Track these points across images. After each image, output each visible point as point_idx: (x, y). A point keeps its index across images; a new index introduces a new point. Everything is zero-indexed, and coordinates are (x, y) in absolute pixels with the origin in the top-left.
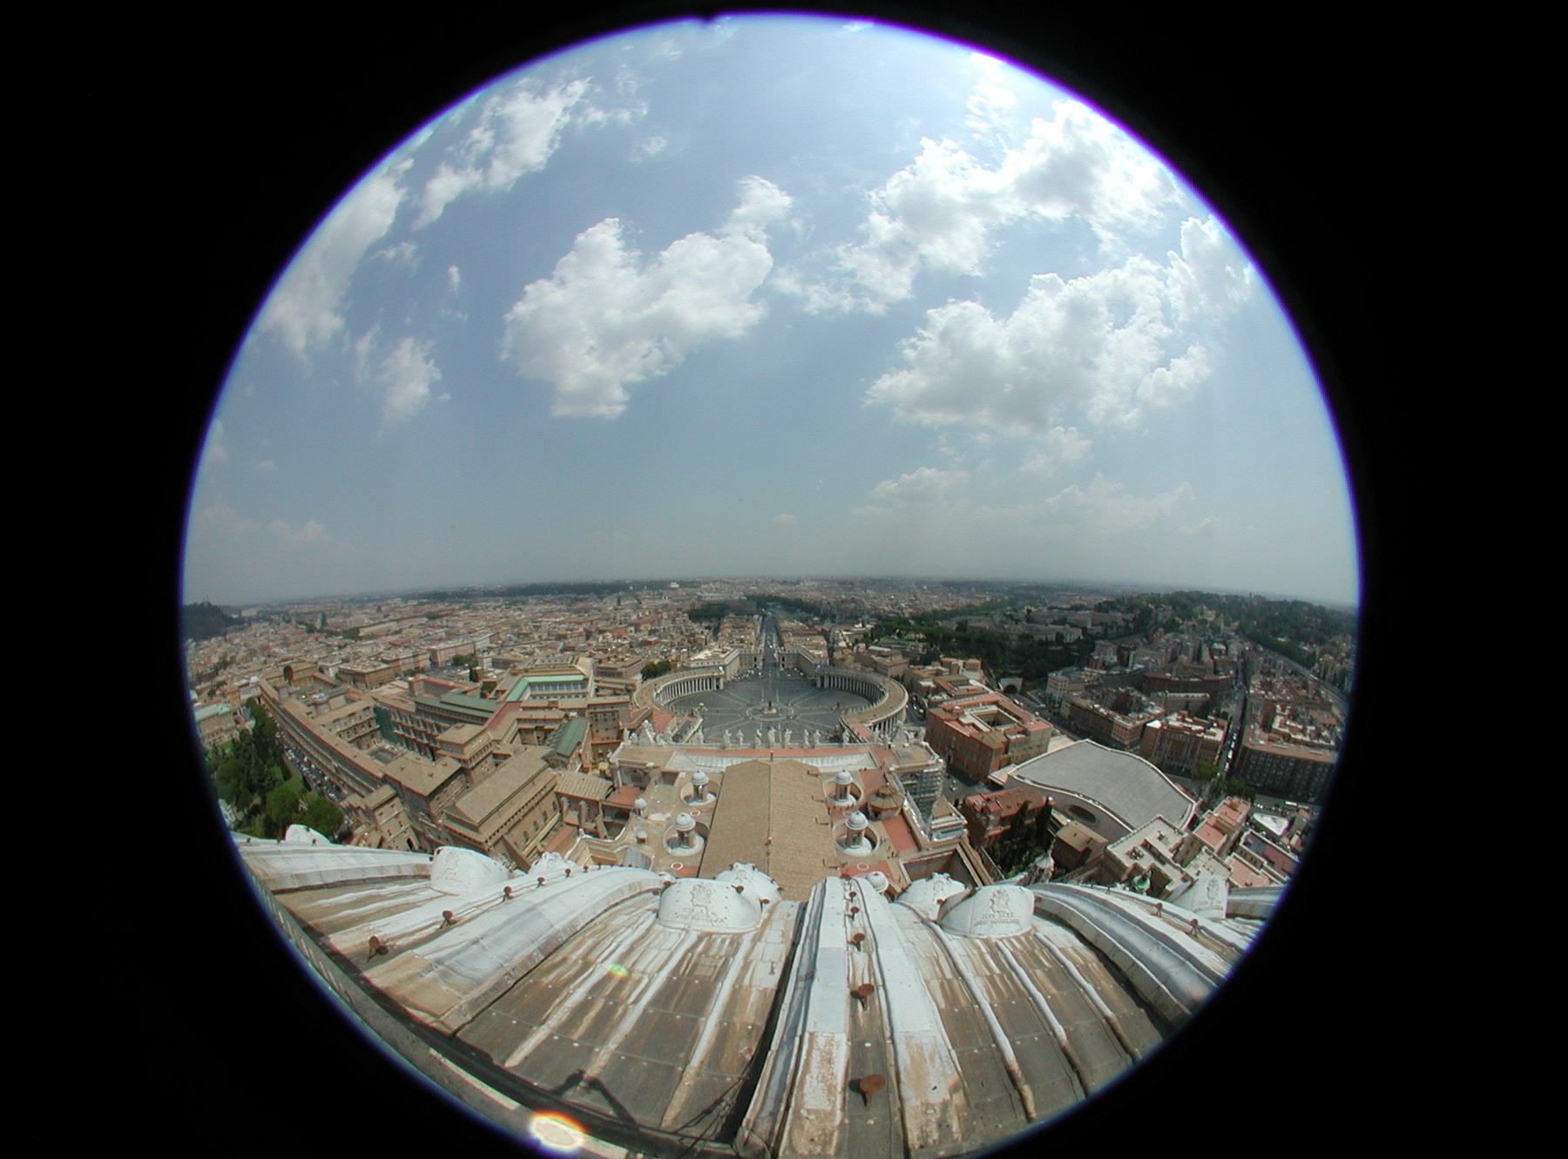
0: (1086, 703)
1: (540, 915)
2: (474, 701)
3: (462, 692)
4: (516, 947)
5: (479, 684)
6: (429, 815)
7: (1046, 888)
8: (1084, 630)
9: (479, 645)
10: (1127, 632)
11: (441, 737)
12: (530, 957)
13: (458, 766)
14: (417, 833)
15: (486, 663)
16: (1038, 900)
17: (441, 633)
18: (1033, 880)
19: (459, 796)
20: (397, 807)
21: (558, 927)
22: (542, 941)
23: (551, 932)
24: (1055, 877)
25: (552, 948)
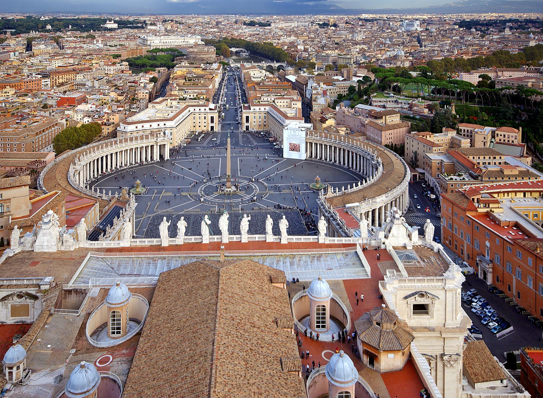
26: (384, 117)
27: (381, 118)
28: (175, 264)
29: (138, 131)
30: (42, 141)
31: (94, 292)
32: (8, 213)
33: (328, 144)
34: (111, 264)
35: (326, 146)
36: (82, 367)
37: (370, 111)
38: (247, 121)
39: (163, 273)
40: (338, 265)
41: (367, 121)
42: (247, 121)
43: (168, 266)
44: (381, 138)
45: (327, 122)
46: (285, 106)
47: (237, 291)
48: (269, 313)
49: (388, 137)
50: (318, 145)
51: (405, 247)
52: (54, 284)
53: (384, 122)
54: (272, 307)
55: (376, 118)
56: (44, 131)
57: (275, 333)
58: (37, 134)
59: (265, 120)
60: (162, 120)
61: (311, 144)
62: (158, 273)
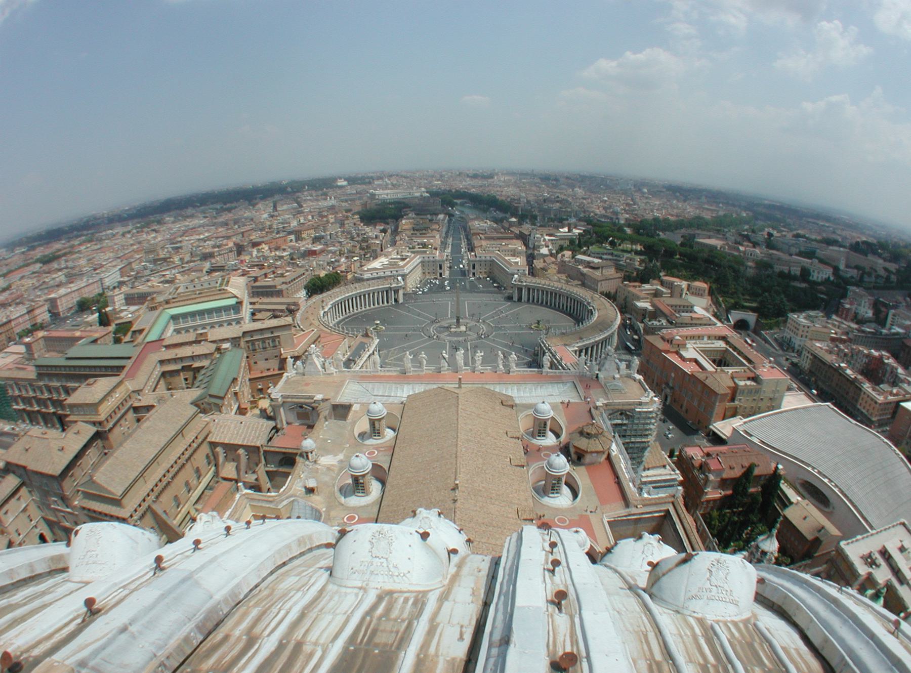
0: (830, 359)
1: (197, 584)
2: (108, 349)
3: (90, 340)
4: (172, 628)
5: (112, 328)
6: (64, 499)
7: (768, 570)
8: (836, 269)
9: (108, 282)
10: (887, 285)
11: (71, 400)
12: (187, 639)
13: (92, 430)
14: (51, 524)
15: (118, 299)
16: (761, 581)
17: (60, 277)
18: (757, 558)
19: (96, 466)
20: (26, 498)
21: (218, 597)
22: (200, 617)
23: (211, 603)
24: (778, 563)
25: (212, 625)
27: (598, 268)
28: (419, 388)
29: (373, 279)
31: (356, 407)
37: (589, 262)
38: (474, 268)
41: (585, 270)
42: (474, 268)
51: (614, 378)
61: (534, 290)
62: (405, 395)
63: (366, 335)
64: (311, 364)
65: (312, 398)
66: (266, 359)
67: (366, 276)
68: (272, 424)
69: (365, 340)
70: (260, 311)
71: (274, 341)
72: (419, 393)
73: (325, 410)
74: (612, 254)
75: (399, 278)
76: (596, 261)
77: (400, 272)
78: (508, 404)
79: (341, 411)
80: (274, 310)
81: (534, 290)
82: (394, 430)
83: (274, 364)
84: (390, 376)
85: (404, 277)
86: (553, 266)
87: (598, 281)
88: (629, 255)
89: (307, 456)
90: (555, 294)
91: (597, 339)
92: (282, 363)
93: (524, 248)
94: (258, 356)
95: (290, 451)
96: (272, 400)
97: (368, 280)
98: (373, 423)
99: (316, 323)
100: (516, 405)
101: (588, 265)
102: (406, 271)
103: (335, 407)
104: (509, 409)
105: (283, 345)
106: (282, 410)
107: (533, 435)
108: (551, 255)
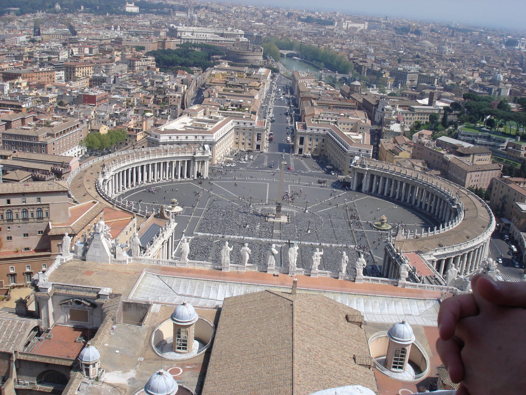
26: (471, 156)
27: (468, 155)
28: (238, 290)
29: (172, 143)
30: (63, 143)
31: (155, 308)
32: (47, 219)
33: (399, 180)
34: (168, 283)
35: (396, 181)
36: (160, 374)
38: (302, 142)
39: (228, 298)
40: (418, 311)
41: (450, 157)
42: (302, 142)
43: (230, 292)
44: (465, 178)
45: (400, 154)
46: (350, 129)
47: (313, 324)
48: (346, 350)
49: (474, 178)
50: (387, 180)
52: (113, 296)
53: (471, 161)
54: (349, 344)
55: (461, 155)
56: (64, 131)
57: (353, 368)
58: (57, 134)
59: (323, 144)
60: (201, 132)
61: (378, 178)
63: (160, 216)
64: (96, 246)
65: (93, 290)
66: (26, 235)
67: (163, 138)
68: (34, 323)
69: (158, 222)
70: (14, 168)
71: (40, 211)
72: (241, 296)
73: (114, 310)
74: (489, 138)
75: (207, 146)
76: (466, 145)
77: (208, 139)
78: (353, 319)
79: (138, 311)
80: (33, 170)
81: (378, 178)
82: (202, 342)
83: (34, 241)
84: (200, 272)
85: (212, 144)
86: (405, 147)
87: (467, 172)
88: (513, 141)
89: (87, 371)
90: (411, 186)
91: (463, 248)
92: (47, 243)
93: (369, 122)
94: (14, 228)
95: (57, 362)
96: (37, 289)
97: (165, 144)
98: (178, 330)
99: (94, 193)
100: (366, 323)
101: (453, 150)
102: (215, 137)
103: (127, 306)
104: (356, 327)
105: (52, 218)
106: (50, 302)
107: (385, 363)
108: (404, 135)
